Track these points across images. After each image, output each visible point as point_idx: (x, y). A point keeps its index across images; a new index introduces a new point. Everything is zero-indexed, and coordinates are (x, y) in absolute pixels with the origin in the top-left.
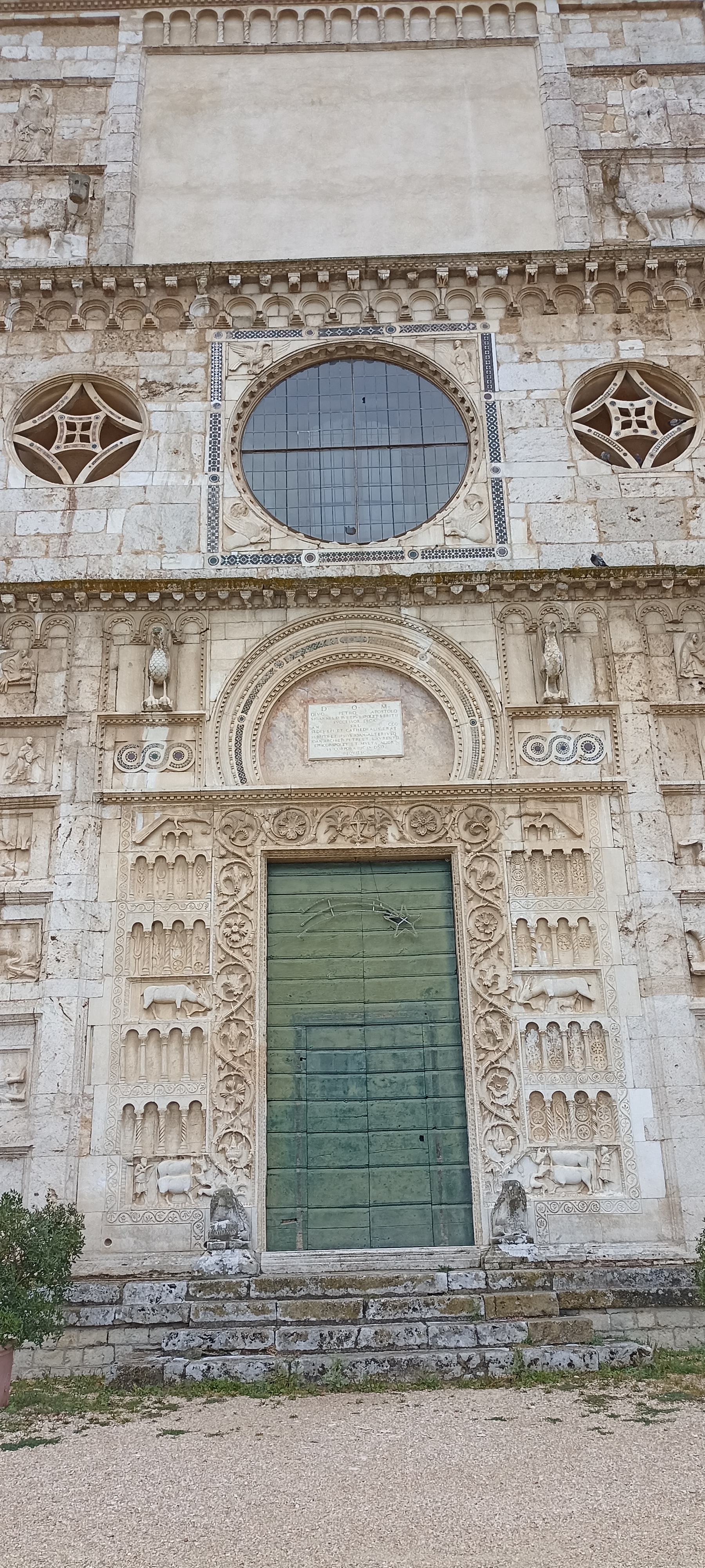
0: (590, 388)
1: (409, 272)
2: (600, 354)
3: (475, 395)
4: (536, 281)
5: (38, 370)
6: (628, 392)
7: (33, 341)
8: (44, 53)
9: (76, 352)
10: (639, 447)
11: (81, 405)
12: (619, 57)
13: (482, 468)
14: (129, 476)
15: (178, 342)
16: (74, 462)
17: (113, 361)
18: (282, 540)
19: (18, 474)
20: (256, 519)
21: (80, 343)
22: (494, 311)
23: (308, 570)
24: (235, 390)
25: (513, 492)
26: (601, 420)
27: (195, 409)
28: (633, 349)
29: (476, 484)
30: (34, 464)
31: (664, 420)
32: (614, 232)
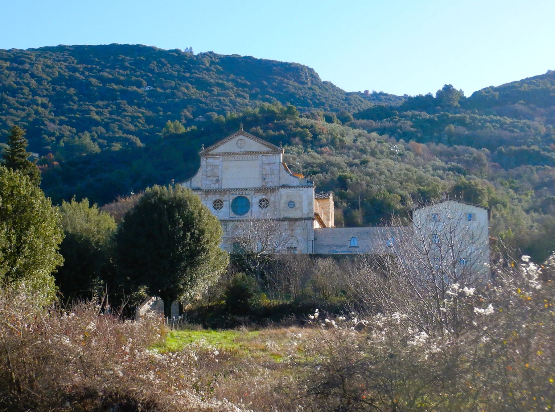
0: (261, 201)
1: (245, 189)
2: (261, 197)
3: (251, 201)
4: (257, 190)
5: (214, 199)
6: (264, 201)
7: (214, 196)
8: (212, 161)
9: (217, 197)
10: (264, 206)
11: (218, 202)
12: (267, 162)
13: (251, 209)
14: (222, 209)
15: (226, 196)
16: (218, 208)
17: (221, 198)
18: (235, 216)
19: (214, 209)
20: (233, 213)
21: (218, 196)
22: (253, 192)
23: (237, 218)
24: (231, 201)
25: (253, 211)
26: (261, 204)
27: (228, 203)
28: (264, 197)
29: (250, 211)
30: (215, 208)
31: (266, 204)
32: (264, 184)
